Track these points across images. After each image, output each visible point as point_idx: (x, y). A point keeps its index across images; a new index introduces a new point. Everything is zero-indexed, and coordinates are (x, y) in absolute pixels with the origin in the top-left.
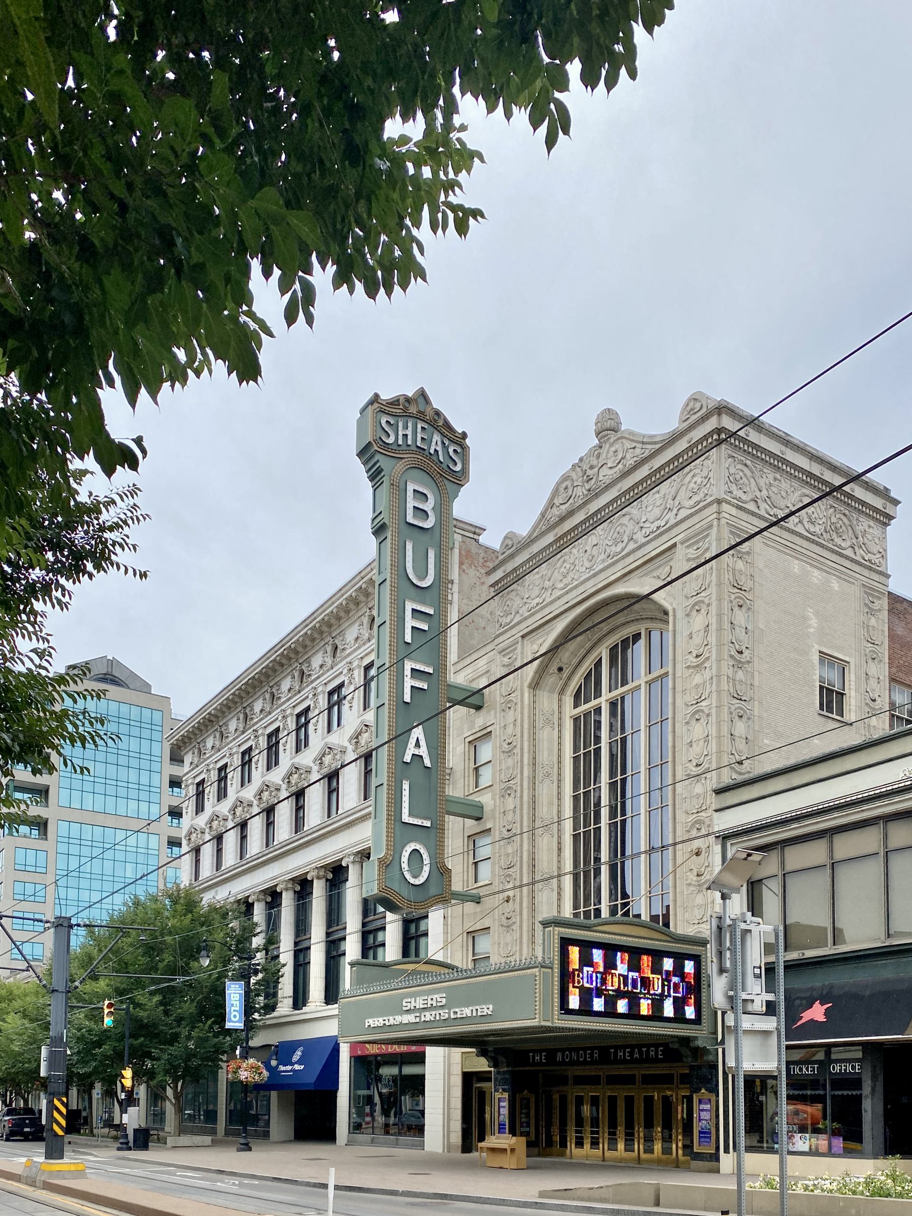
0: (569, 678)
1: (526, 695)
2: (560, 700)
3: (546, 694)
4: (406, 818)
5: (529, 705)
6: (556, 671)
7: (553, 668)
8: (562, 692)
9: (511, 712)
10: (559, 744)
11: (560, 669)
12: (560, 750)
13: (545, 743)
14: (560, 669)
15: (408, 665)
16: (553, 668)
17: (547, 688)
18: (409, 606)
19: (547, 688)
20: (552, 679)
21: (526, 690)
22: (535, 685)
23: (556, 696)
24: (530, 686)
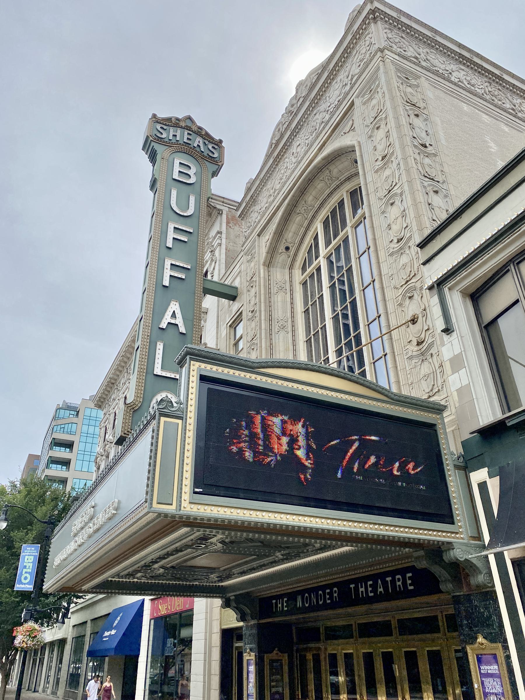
0: (296, 255)
1: (262, 271)
2: (290, 273)
3: (278, 270)
4: (158, 371)
5: (264, 277)
6: (284, 250)
7: (282, 248)
8: (291, 267)
9: (253, 289)
10: (292, 303)
11: (287, 249)
12: (292, 308)
13: (280, 304)
14: (287, 249)
15: (168, 263)
16: (282, 248)
17: (279, 265)
18: (171, 226)
19: (279, 265)
20: (282, 258)
21: (262, 267)
22: (269, 264)
23: (287, 271)
24: (264, 264)
